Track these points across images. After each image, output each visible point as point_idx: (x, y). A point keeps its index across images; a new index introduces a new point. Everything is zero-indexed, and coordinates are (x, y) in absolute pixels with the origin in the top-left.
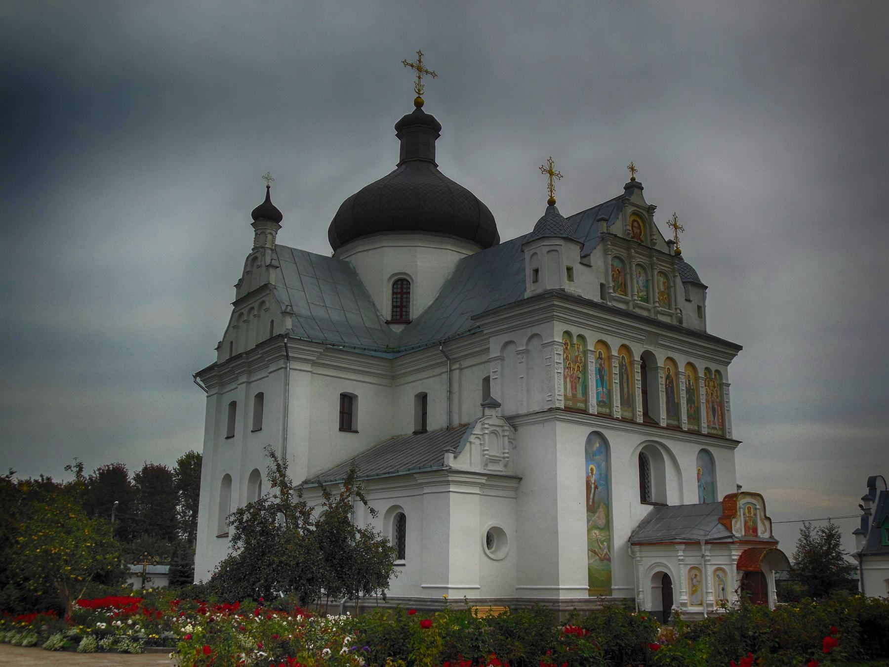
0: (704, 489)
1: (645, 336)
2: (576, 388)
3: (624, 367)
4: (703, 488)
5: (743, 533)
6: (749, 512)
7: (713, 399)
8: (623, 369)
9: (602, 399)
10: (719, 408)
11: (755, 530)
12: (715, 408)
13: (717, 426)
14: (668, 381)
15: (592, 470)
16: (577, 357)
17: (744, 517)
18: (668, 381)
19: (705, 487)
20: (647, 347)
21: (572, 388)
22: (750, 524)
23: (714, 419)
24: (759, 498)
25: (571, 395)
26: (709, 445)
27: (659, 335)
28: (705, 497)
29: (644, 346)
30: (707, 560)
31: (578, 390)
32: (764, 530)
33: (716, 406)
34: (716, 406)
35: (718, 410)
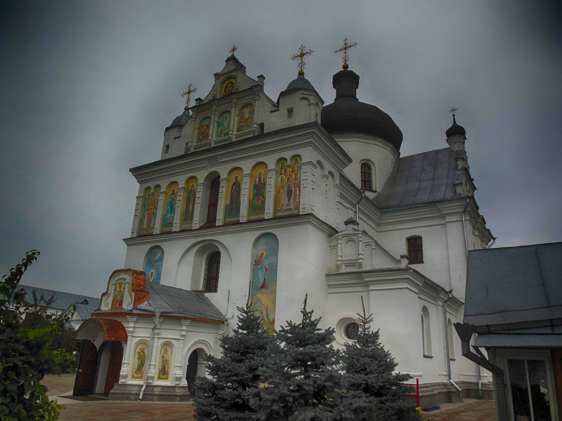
0: (266, 270)
1: (206, 163)
2: (150, 221)
3: (192, 192)
4: (264, 270)
5: (110, 306)
6: (120, 287)
7: (289, 183)
8: (191, 194)
9: (169, 222)
10: (298, 189)
11: (121, 303)
12: (292, 191)
13: (292, 207)
14: (234, 187)
15: (152, 273)
16: (155, 200)
17: (114, 292)
18: (234, 187)
19: (267, 268)
20: (211, 170)
21: (148, 222)
22: (119, 298)
23: (289, 201)
24: (116, 274)
25: (146, 226)
26: (271, 228)
27: (216, 156)
28: (266, 278)
29: (209, 170)
30: (155, 333)
31: (152, 222)
32: (130, 302)
33: (293, 189)
34: (293, 189)
35: (295, 190)
